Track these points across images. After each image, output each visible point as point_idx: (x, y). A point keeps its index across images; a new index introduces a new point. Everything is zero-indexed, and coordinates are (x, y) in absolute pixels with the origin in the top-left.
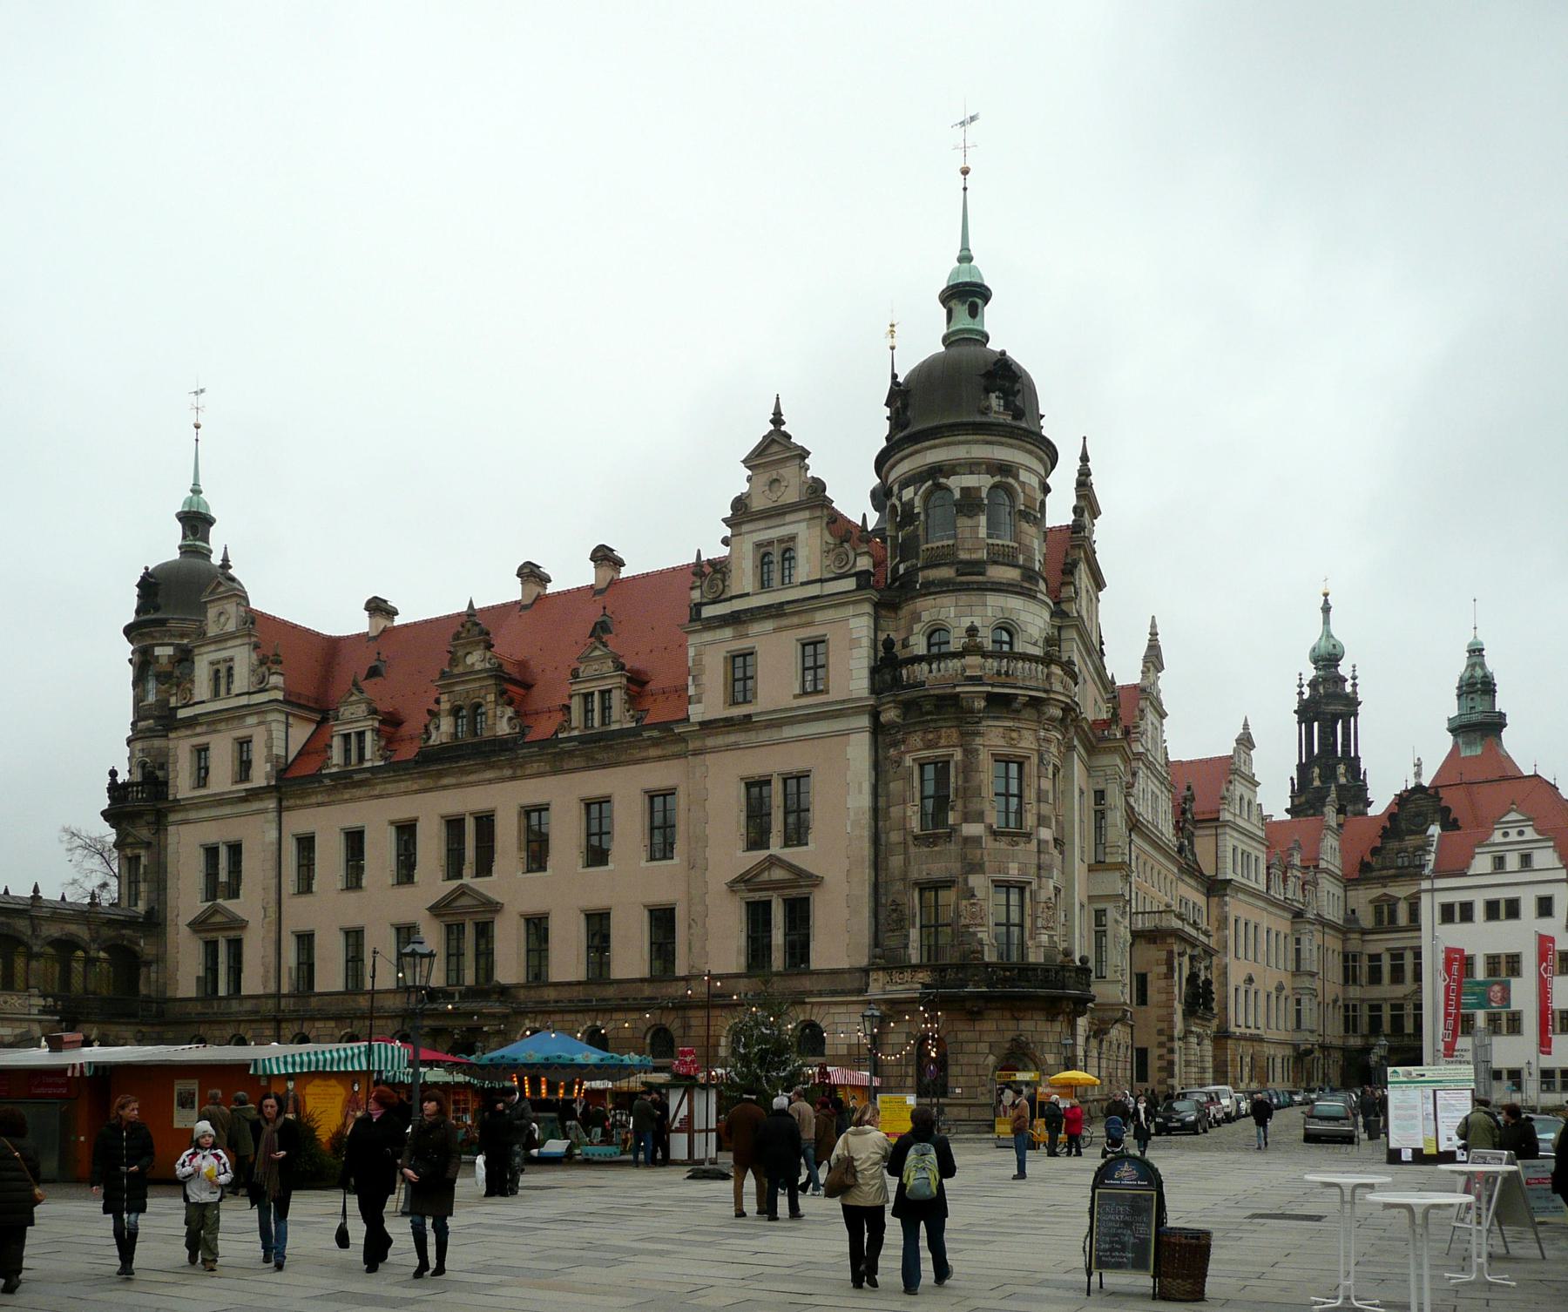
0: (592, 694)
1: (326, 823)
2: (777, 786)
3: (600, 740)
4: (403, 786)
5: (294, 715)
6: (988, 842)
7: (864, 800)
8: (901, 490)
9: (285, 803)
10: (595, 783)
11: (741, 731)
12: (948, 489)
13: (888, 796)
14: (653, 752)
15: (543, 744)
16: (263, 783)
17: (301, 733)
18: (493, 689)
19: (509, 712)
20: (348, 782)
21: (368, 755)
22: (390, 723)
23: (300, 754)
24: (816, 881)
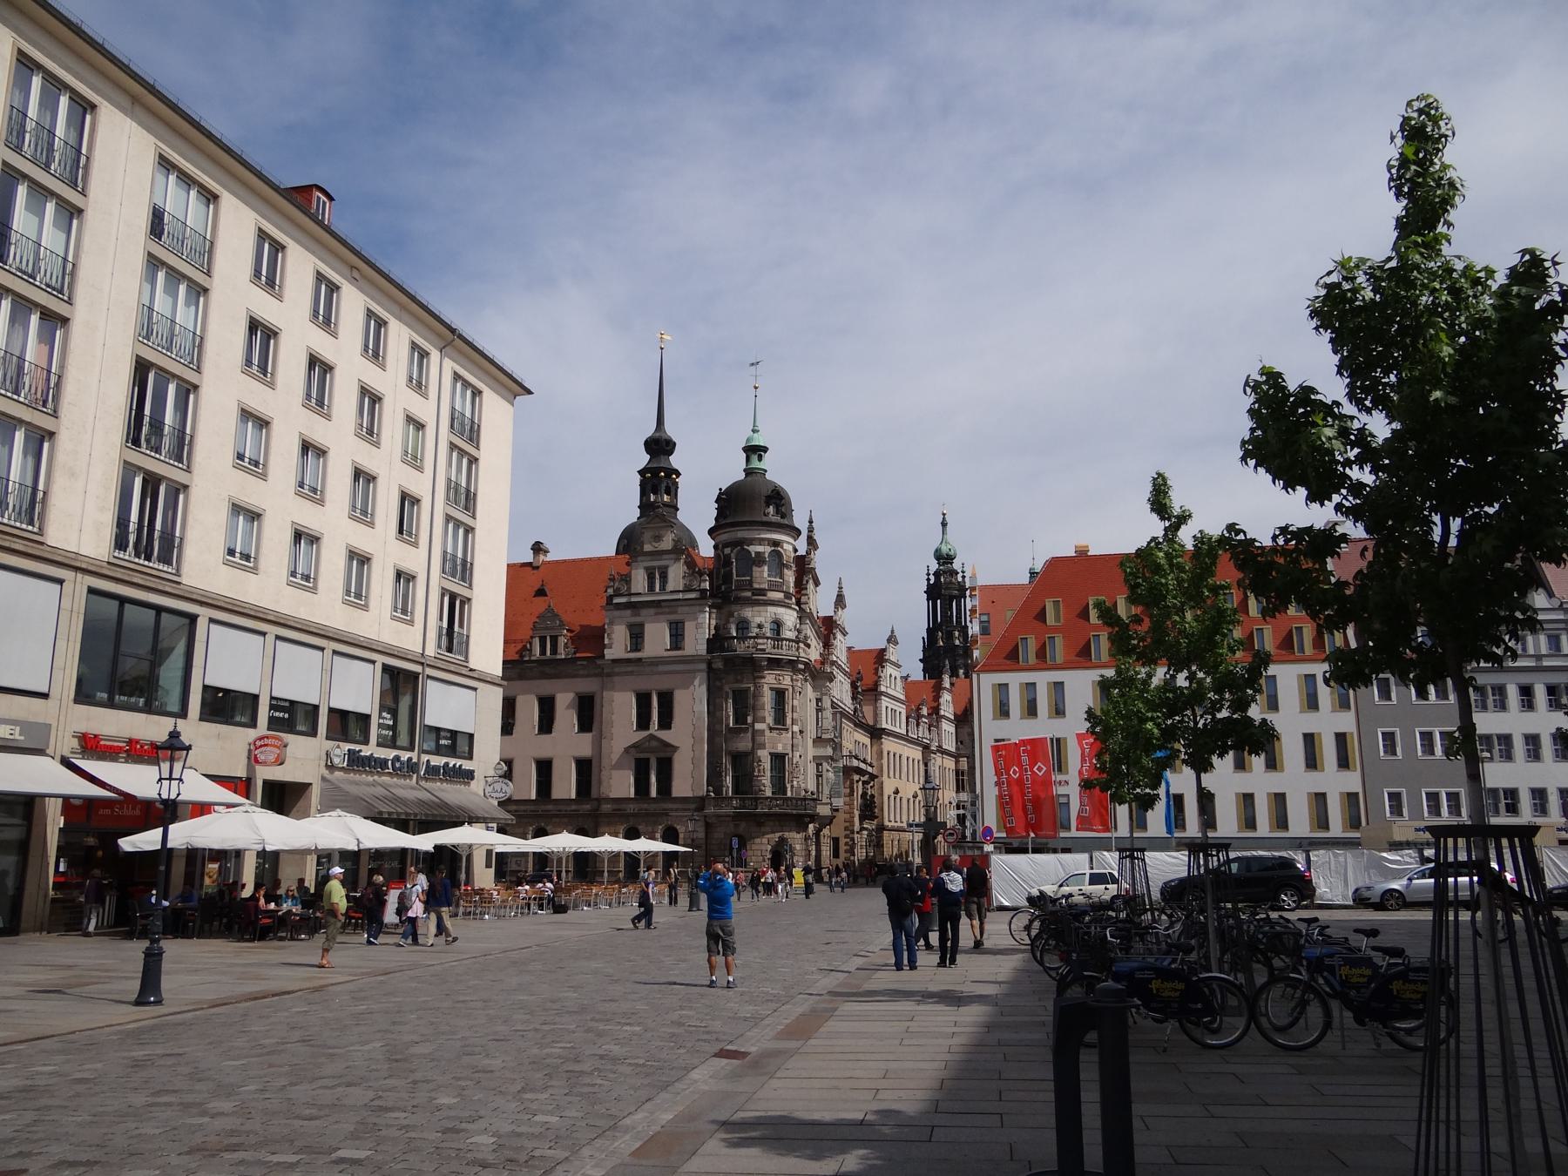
6: (767, 732)
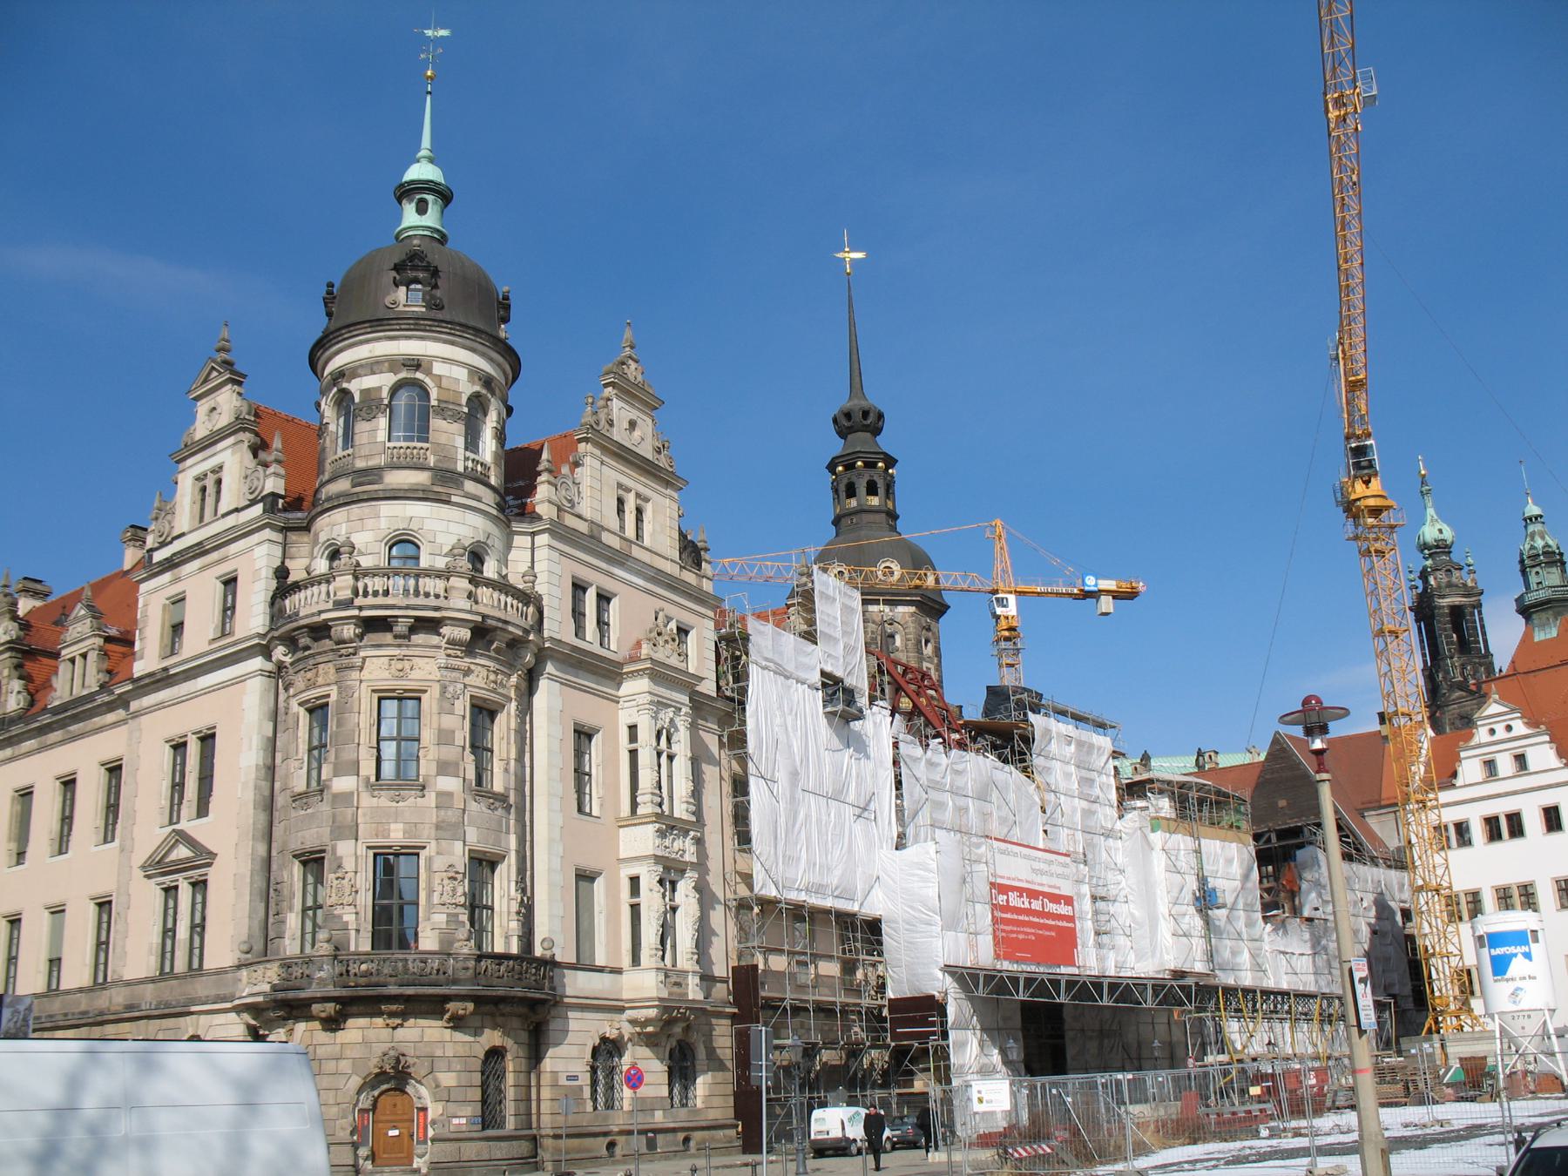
6: (367, 801)
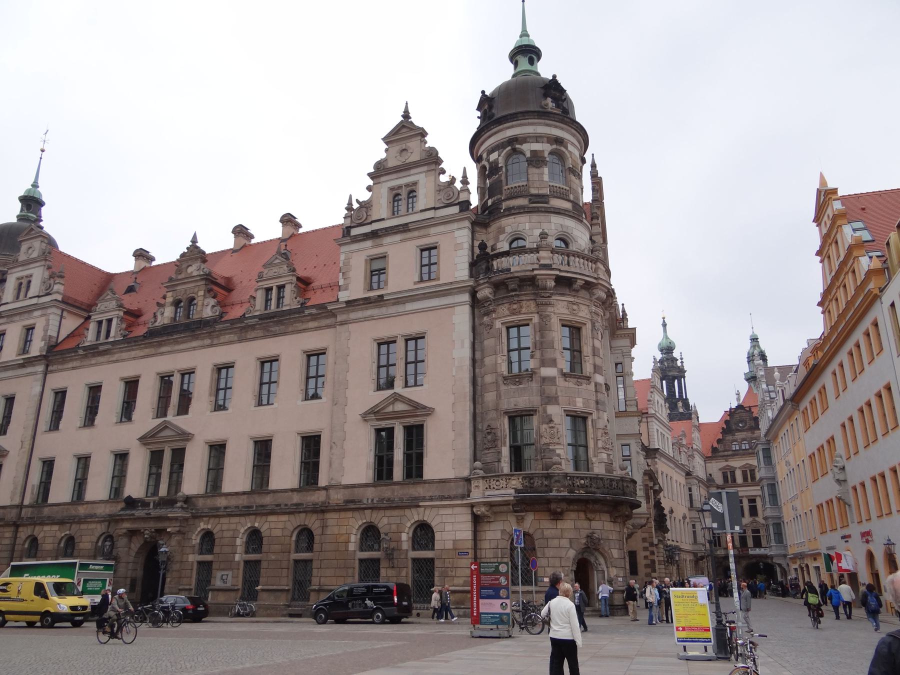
0: (271, 289)
1: (75, 381)
2: (401, 343)
3: (273, 317)
4: (133, 354)
5: (69, 312)
6: (560, 381)
7: (466, 353)
8: (488, 155)
9: (50, 368)
10: (267, 347)
11: (375, 307)
12: (522, 153)
13: (482, 351)
14: (312, 324)
15: (233, 322)
16: (38, 354)
17: (71, 324)
18: (203, 287)
19: (212, 302)
20: (94, 351)
21: (112, 333)
22: (133, 316)
23: (68, 336)
24: (428, 411)
